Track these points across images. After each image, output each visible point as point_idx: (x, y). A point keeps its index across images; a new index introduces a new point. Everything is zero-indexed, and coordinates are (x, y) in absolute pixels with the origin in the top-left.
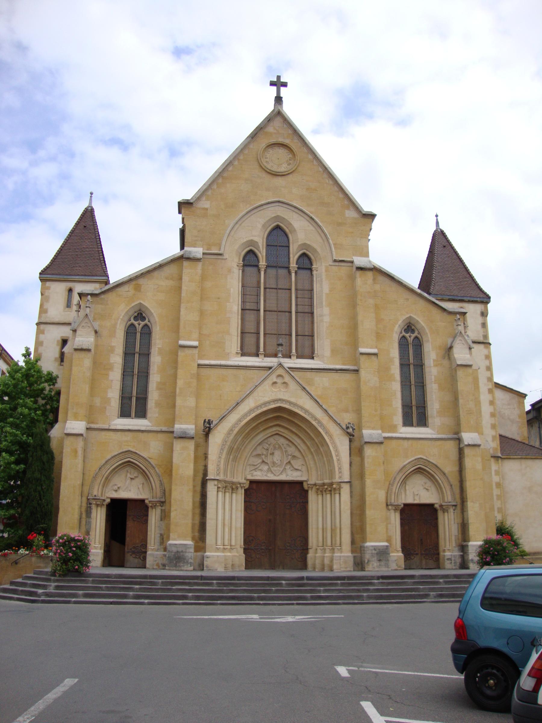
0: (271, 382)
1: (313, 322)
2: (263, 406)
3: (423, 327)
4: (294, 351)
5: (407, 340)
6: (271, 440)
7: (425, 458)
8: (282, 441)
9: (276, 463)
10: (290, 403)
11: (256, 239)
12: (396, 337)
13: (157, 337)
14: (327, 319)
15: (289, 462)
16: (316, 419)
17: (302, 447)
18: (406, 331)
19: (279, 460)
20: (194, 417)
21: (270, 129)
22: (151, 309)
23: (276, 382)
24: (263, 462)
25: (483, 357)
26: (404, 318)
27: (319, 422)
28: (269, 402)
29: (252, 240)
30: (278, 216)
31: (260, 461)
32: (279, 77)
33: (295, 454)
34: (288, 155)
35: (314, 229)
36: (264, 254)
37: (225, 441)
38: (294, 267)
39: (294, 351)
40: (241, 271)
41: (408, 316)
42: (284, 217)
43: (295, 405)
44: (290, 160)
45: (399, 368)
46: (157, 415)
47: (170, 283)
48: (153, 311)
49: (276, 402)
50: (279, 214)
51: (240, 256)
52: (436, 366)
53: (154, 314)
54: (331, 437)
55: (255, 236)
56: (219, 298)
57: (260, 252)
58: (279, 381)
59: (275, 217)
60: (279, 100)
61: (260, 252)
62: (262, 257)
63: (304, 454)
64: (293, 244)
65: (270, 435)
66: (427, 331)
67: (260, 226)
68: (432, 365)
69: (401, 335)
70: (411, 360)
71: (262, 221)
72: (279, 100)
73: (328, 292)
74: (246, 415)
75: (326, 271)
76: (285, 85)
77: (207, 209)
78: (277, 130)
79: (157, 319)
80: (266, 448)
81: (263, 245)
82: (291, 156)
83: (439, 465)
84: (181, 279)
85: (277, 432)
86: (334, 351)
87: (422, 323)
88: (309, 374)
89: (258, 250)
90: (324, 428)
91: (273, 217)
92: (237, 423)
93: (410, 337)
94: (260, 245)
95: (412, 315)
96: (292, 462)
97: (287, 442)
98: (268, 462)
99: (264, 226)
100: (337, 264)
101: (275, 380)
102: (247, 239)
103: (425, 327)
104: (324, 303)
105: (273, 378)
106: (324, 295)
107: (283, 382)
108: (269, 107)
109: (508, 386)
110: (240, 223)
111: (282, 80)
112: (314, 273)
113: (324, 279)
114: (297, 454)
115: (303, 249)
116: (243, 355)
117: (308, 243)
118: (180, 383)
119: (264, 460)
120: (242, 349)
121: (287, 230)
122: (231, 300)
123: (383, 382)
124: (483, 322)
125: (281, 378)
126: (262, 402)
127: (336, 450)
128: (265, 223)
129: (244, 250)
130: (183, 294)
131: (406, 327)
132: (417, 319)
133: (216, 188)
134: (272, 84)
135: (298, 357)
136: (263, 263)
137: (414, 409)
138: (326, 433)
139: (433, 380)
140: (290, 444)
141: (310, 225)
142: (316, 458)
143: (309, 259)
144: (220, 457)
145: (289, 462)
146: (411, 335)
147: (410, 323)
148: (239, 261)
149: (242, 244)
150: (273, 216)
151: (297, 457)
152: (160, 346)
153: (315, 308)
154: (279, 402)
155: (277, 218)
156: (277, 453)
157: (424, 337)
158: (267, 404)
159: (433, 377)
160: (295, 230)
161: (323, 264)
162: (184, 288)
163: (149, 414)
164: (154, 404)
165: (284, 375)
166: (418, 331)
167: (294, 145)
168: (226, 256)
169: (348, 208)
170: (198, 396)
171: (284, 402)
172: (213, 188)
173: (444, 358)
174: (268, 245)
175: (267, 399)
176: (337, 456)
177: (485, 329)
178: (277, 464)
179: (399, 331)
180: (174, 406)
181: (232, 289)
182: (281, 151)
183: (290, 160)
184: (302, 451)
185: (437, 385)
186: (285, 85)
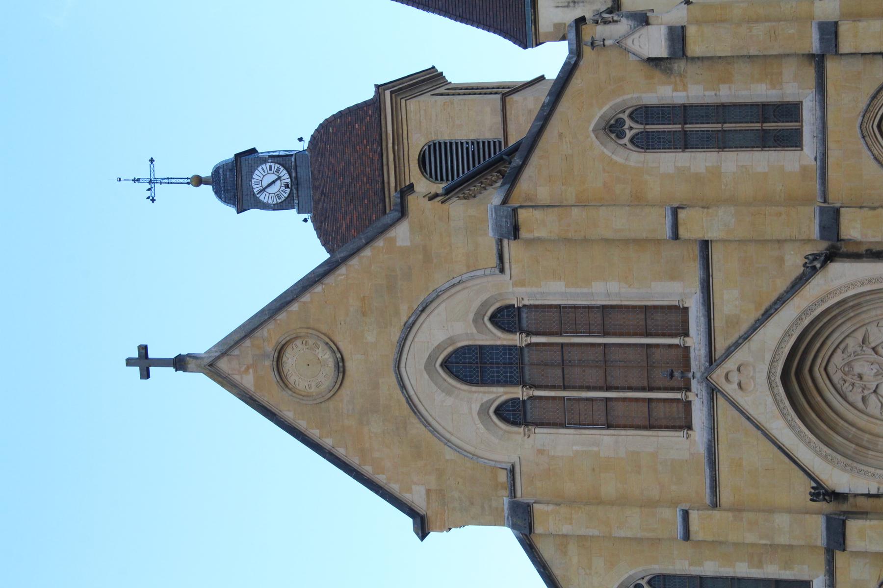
0: (739, 391)
1: (620, 307)
2: (782, 405)
4: (675, 341)
5: (637, 134)
6: (836, 378)
7: (860, 118)
8: (838, 360)
9: (876, 372)
10: (773, 361)
11: (476, 407)
12: (636, 158)
13: (671, 567)
14: (614, 287)
15: (874, 349)
16: (800, 318)
17: (847, 328)
18: (621, 135)
19: (872, 367)
20: (807, 516)
21: (248, 381)
22: (622, 579)
23: (738, 384)
24: (875, 391)
26: (598, 143)
27: (805, 313)
28: (774, 396)
29: (479, 414)
30: (426, 368)
31: (873, 397)
32: (130, 362)
33: (861, 339)
34: (297, 347)
35: (443, 306)
36: (501, 390)
37: (845, 468)
38: (521, 340)
39: (675, 341)
40: (538, 430)
41: (593, 135)
42: (427, 357)
43: (776, 352)
44: (307, 343)
45: (693, 154)
46: (806, 567)
47: (573, 548)
48: (626, 576)
49: (774, 385)
50: (423, 368)
51: (509, 432)
53: (631, 573)
54: (830, 293)
55: (470, 409)
56: (593, 470)
57: (498, 397)
58: (735, 377)
59: (429, 374)
60: (180, 363)
61: (500, 396)
62: (506, 393)
63: (858, 326)
64: (475, 340)
65: (828, 382)
66: (619, 100)
67: (450, 401)
68: (684, 94)
69: (629, 146)
70: (677, 127)
71: (439, 396)
72: (180, 363)
73: (563, 283)
74: (799, 434)
75: (523, 285)
76: (143, 349)
77: (428, 491)
78: (247, 369)
79: (641, 569)
80: (851, 388)
81: (484, 393)
82: (298, 342)
83: (872, 91)
84: (565, 536)
85: (822, 369)
86: (673, 276)
87: (605, 109)
88: (719, 323)
89: (494, 400)
90: (816, 304)
91: (429, 376)
92: (814, 449)
93: (631, 128)
94: (486, 398)
95: (591, 128)
96: (873, 345)
97: (839, 351)
98: (876, 384)
99: (449, 393)
100: (507, 266)
101: (735, 386)
102: (478, 421)
103: (611, 103)
104: (585, 290)
105: (731, 389)
106: (568, 290)
107: (736, 373)
108: (200, 381)
110: (448, 436)
111: (136, 355)
112: (526, 302)
113: (540, 290)
114: (859, 335)
115: (484, 323)
116: (690, 427)
117: (471, 316)
118: (751, 538)
119: (872, 391)
120: (680, 428)
121: (450, 349)
122: (595, 449)
123: (723, 187)
125: (729, 376)
126: (775, 407)
127: (853, 285)
128: (443, 391)
129: (496, 424)
130: (596, 532)
131: (613, 136)
132: (597, 118)
133: (384, 476)
134: (145, 375)
135: (686, 334)
136: (518, 393)
137: (768, 126)
138: (823, 301)
139: (713, 93)
140: (842, 346)
141: (436, 312)
142: (865, 309)
143: (500, 310)
144: (873, 475)
145: (874, 349)
146: (627, 126)
147: (605, 129)
148: (520, 433)
149: (487, 429)
150: (426, 376)
151: (865, 335)
152: (687, 563)
153: (593, 303)
154: (772, 378)
155: (429, 366)
156: (858, 368)
157: (630, 104)
158: (778, 398)
159: (707, 93)
160: (450, 338)
161: (511, 290)
162: (583, 531)
163: (805, 578)
164: (787, 572)
165: (725, 371)
166: (620, 113)
167: (271, 334)
168: (514, 459)
169: (394, 240)
170: (771, 510)
171: (773, 370)
172: (385, 481)
173: (671, 70)
174: (483, 382)
175: (770, 400)
176: (863, 284)
178: (878, 371)
179: (621, 150)
180: (791, 547)
181: (575, 448)
182: (290, 360)
183: (307, 343)
184: (854, 328)
185: (721, 86)
186: (143, 349)
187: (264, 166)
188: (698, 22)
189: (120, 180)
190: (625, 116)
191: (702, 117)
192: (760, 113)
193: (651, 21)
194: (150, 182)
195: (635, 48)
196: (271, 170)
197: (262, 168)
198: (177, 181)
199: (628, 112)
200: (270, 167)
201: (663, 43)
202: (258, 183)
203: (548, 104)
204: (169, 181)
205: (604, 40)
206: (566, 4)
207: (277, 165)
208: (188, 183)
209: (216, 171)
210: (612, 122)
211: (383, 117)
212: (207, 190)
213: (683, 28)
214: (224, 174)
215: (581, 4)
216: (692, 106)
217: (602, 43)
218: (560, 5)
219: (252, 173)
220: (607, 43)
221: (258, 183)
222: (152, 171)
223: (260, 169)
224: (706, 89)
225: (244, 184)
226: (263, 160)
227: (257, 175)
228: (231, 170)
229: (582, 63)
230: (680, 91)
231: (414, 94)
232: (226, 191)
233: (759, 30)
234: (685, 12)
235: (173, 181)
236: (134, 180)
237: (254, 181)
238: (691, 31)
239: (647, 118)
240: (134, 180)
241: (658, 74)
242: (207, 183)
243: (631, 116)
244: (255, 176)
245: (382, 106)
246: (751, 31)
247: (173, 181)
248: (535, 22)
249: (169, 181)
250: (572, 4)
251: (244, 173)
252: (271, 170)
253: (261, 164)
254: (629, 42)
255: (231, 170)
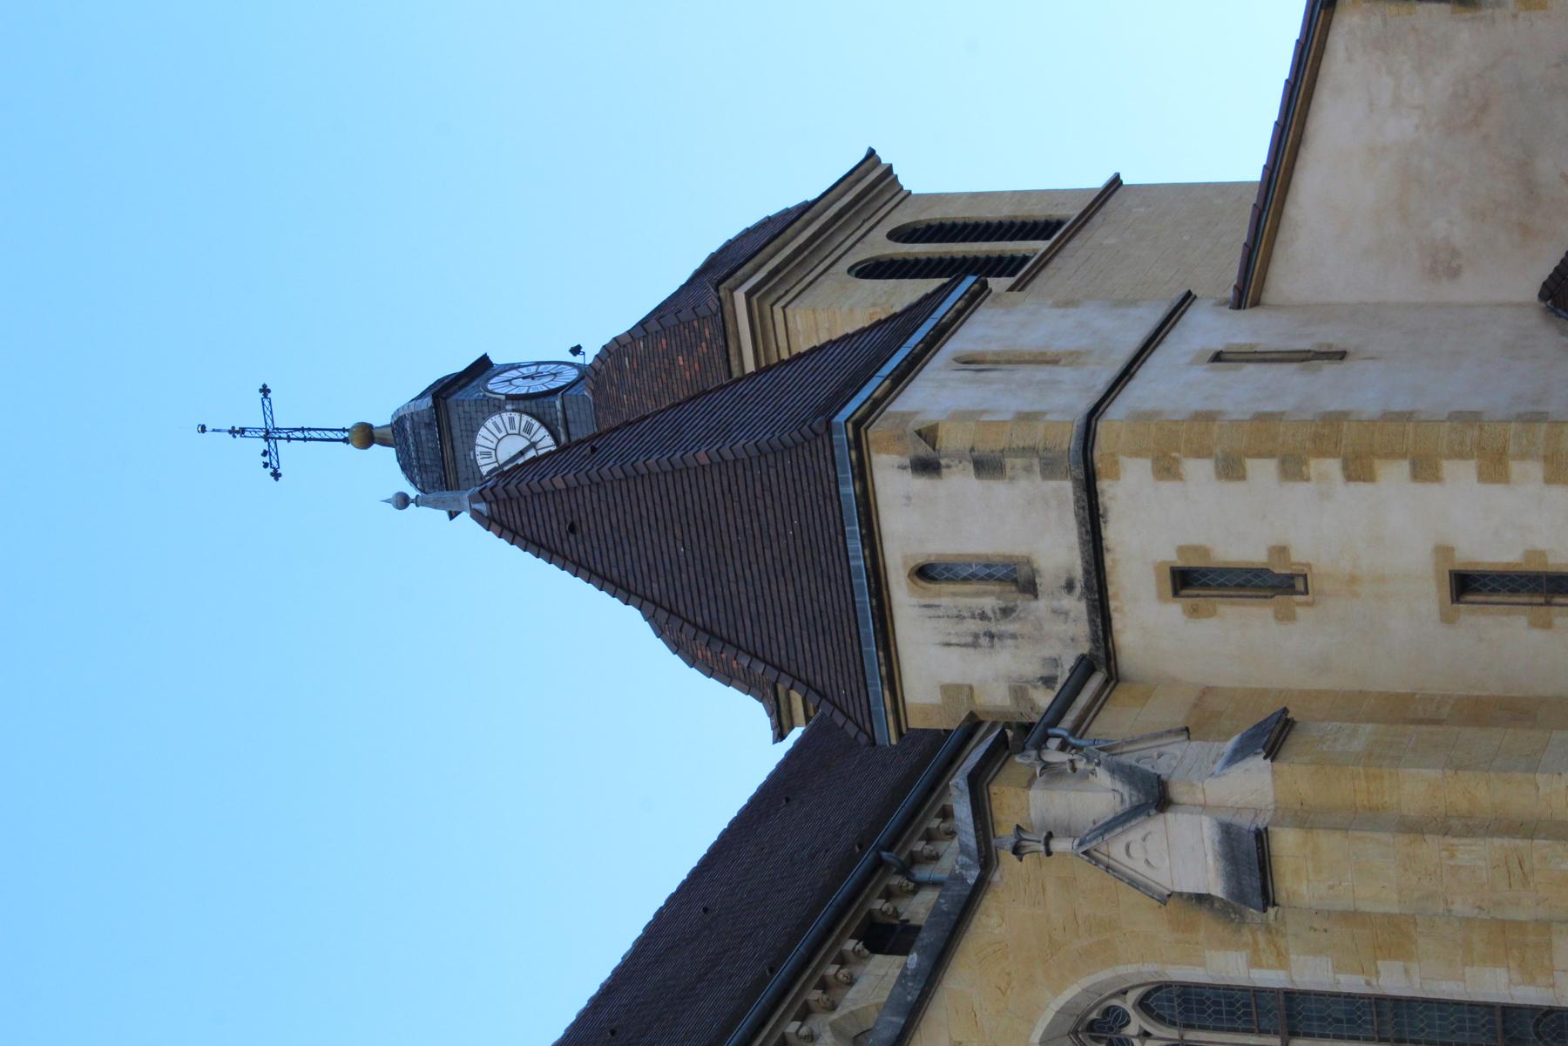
3: (1086, 991)
25: (1168, 487)
52: (1282, 960)
66: (1104, 975)
103: (1086, 982)
109: (1284, 71)
124: (971, 467)
146: (1131, 1030)
157: (1136, 982)
159: (1342, 978)
177: (1008, 462)
187: (496, 418)
188: (1305, 819)
189: (203, 429)
190: (1128, 1004)
191: (1339, 1021)
192: (1499, 1026)
193: (1177, 791)
194: (266, 438)
195: (1135, 865)
196: (513, 427)
197: (495, 425)
198: (323, 435)
199: (1133, 996)
200: (511, 420)
201: (1210, 860)
202: (488, 455)
203: (914, 976)
204: (305, 434)
205: (1050, 836)
206: (970, 639)
207: (526, 418)
208: (345, 440)
209: (399, 424)
210: (1093, 1016)
211: (733, 350)
212: (384, 458)
213: (1261, 836)
214: (416, 434)
215: (1010, 642)
216: (1306, 994)
217: (1042, 848)
218: (954, 640)
219: (474, 432)
220: (1058, 845)
221: (488, 455)
222: (268, 412)
223: (489, 424)
224: (1338, 969)
225: (459, 455)
226: (496, 406)
227: (485, 437)
228: (428, 425)
229: (996, 877)
230: (1269, 967)
231: (812, 270)
232: (423, 468)
233: (1476, 854)
234: (1268, 777)
235: (314, 434)
236: (233, 432)
237: (478, 449)
238: (1285, 842)
239: (1188, 1010)
240: (233, 432)
241: (1206, 924)
242: (384, 443)
243: (1143, 1005)
244: (479, 440)
245: (730, 328)
246: (1452, 856)
247: (314, 434)
248: (892, 680)
249: (305, 434)
250: (984, 641)
251: (456, 432)
252: (513, 427)
253: (491, 414)
254: (1115, 849)
255: (428, 425)
